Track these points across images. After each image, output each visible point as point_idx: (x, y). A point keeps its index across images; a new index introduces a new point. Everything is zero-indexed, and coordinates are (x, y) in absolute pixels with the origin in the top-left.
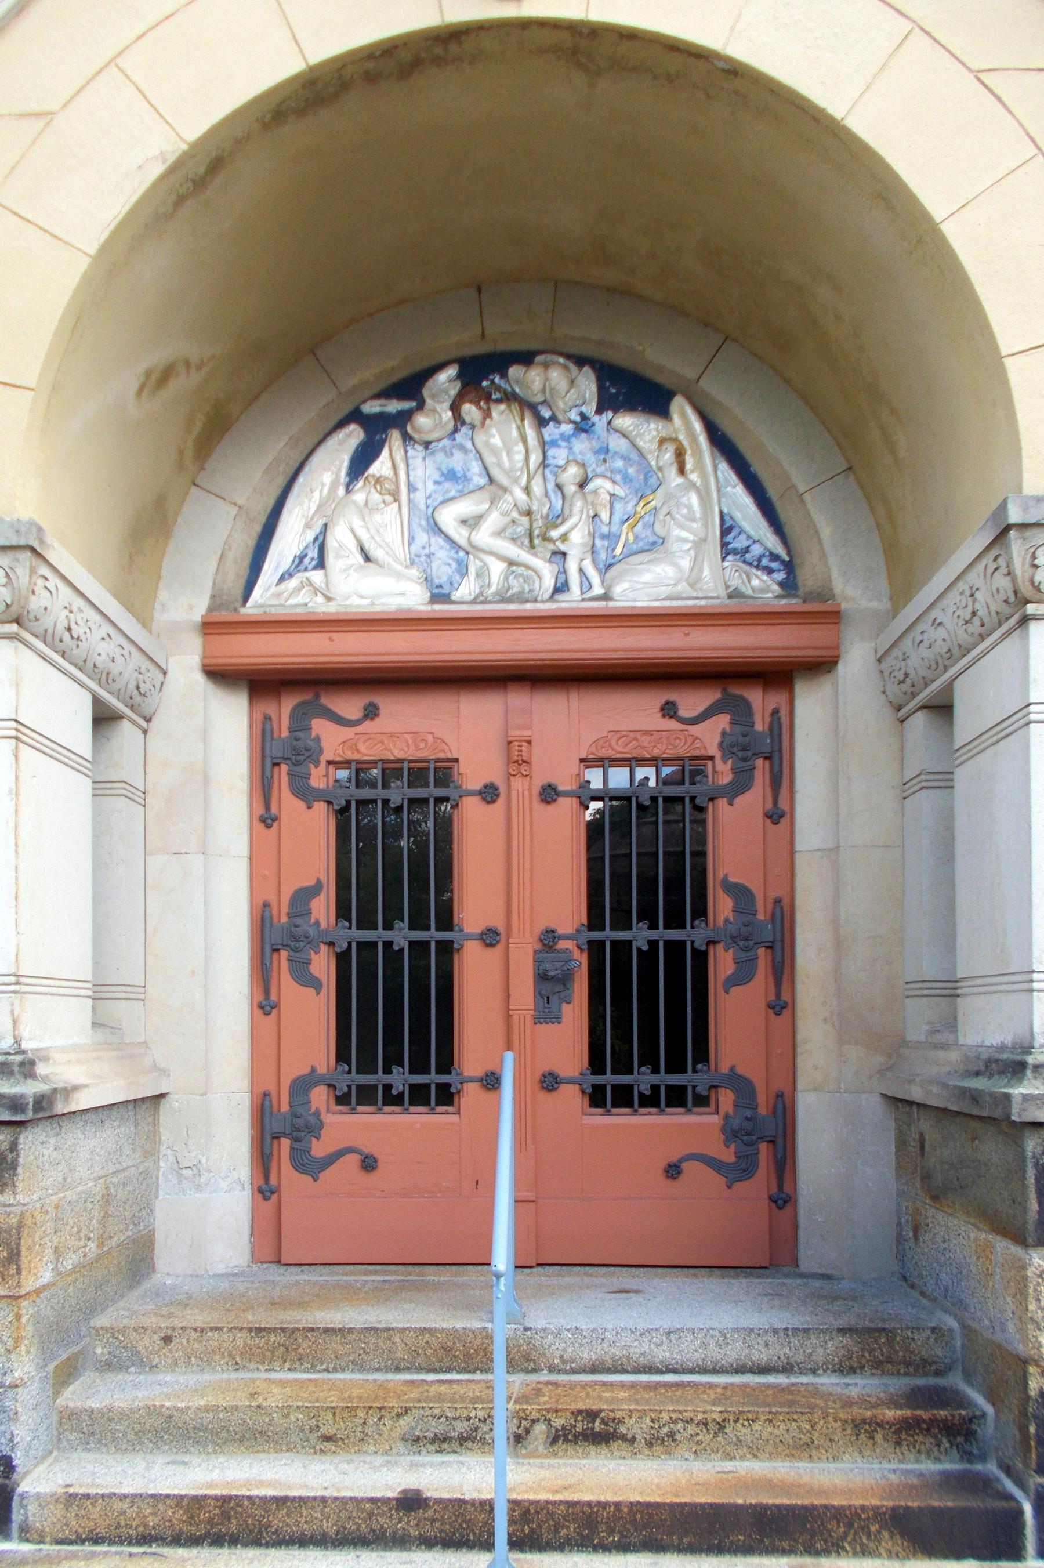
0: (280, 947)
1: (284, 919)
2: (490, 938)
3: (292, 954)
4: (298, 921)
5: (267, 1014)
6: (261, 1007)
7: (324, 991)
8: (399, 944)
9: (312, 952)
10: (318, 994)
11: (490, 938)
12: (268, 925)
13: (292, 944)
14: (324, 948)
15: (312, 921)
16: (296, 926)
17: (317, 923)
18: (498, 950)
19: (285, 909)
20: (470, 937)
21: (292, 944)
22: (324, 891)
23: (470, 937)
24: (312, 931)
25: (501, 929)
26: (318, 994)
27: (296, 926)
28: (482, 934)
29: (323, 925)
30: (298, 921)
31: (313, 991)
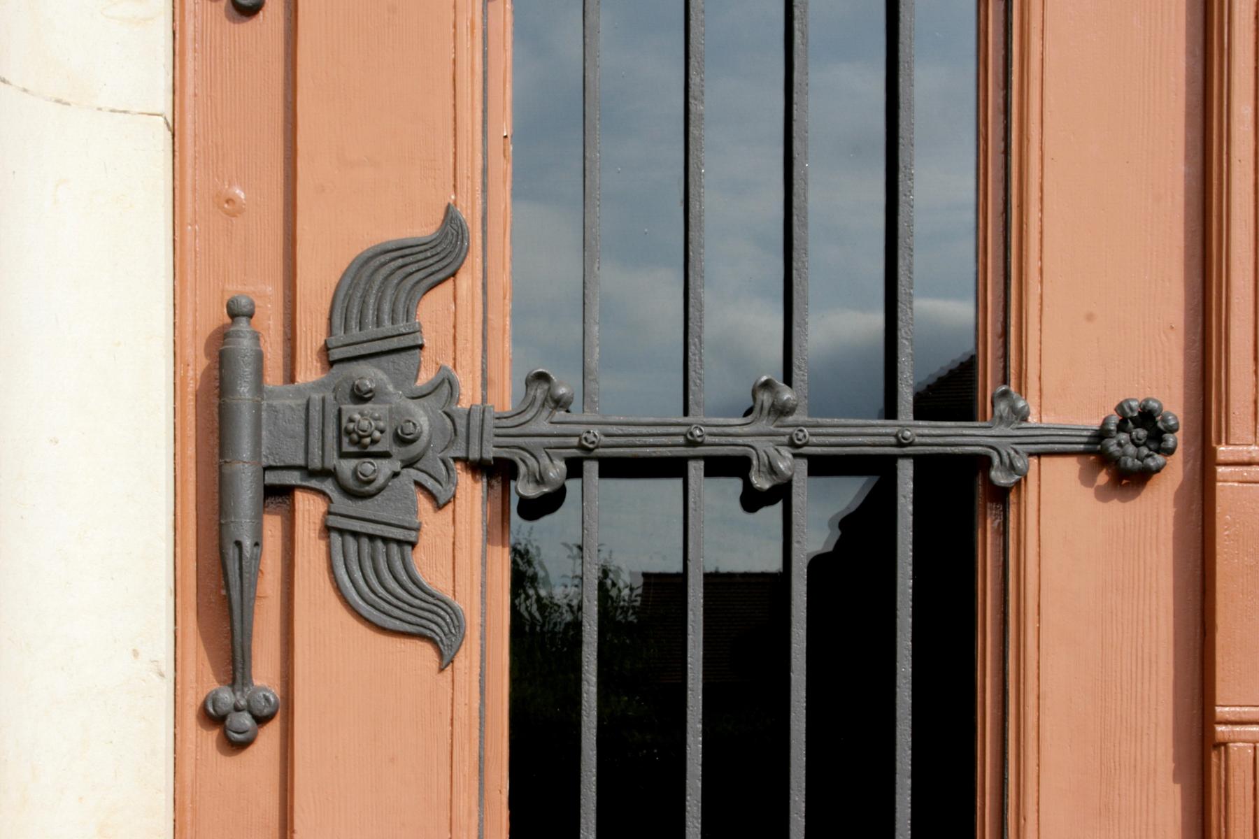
0: (293, 478)
1: (309, 371)
2: (1120, 454)
3: (342, 504)
4: (370, 375)
5: (235, 745)
6: (213, 718)
7: (467, 660)
8: (772, 470)
9: (424, 504)
10: (446, 661)
11: (1120, 454)
12: (244, 390)
13: (346, 467)
14: (471, 493)
15: (426, 377)
16: (360, 396)
17: (446, 384)
18: (1160, 502)
19: (312, 333)
20: (1050, 448)
21: (346, 467)
22: (474, 260)
23: (1050, 448)
24: (423, 419)
25: (1173, 403)
26: (446, 661)
27: (360, 396)
28: (1102, 434)
29: (469, 395)
30: (370, 375)
31: (425, 652)
